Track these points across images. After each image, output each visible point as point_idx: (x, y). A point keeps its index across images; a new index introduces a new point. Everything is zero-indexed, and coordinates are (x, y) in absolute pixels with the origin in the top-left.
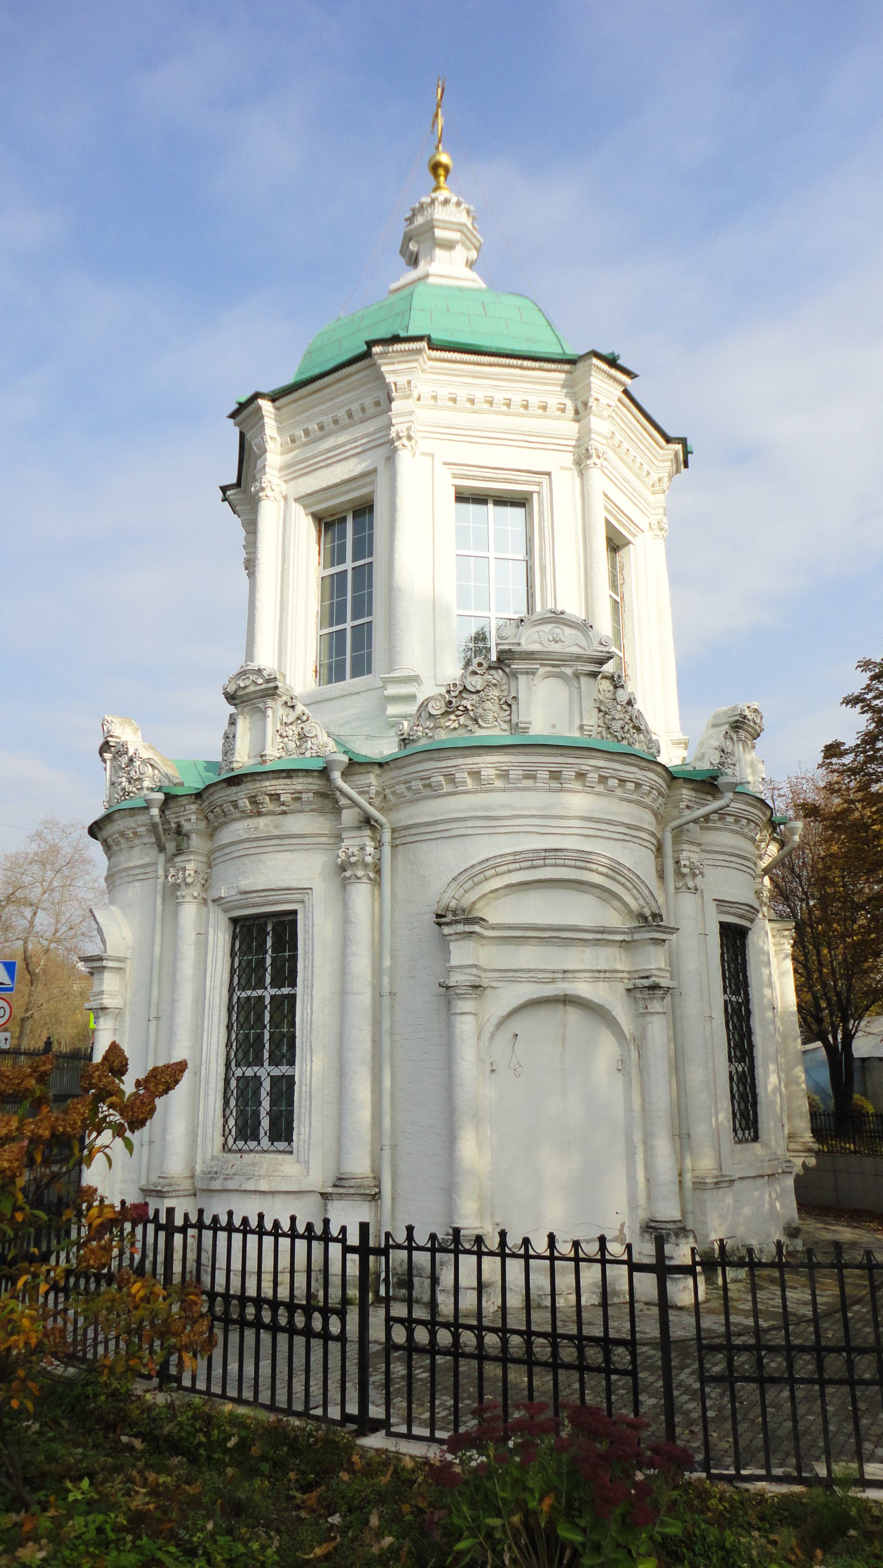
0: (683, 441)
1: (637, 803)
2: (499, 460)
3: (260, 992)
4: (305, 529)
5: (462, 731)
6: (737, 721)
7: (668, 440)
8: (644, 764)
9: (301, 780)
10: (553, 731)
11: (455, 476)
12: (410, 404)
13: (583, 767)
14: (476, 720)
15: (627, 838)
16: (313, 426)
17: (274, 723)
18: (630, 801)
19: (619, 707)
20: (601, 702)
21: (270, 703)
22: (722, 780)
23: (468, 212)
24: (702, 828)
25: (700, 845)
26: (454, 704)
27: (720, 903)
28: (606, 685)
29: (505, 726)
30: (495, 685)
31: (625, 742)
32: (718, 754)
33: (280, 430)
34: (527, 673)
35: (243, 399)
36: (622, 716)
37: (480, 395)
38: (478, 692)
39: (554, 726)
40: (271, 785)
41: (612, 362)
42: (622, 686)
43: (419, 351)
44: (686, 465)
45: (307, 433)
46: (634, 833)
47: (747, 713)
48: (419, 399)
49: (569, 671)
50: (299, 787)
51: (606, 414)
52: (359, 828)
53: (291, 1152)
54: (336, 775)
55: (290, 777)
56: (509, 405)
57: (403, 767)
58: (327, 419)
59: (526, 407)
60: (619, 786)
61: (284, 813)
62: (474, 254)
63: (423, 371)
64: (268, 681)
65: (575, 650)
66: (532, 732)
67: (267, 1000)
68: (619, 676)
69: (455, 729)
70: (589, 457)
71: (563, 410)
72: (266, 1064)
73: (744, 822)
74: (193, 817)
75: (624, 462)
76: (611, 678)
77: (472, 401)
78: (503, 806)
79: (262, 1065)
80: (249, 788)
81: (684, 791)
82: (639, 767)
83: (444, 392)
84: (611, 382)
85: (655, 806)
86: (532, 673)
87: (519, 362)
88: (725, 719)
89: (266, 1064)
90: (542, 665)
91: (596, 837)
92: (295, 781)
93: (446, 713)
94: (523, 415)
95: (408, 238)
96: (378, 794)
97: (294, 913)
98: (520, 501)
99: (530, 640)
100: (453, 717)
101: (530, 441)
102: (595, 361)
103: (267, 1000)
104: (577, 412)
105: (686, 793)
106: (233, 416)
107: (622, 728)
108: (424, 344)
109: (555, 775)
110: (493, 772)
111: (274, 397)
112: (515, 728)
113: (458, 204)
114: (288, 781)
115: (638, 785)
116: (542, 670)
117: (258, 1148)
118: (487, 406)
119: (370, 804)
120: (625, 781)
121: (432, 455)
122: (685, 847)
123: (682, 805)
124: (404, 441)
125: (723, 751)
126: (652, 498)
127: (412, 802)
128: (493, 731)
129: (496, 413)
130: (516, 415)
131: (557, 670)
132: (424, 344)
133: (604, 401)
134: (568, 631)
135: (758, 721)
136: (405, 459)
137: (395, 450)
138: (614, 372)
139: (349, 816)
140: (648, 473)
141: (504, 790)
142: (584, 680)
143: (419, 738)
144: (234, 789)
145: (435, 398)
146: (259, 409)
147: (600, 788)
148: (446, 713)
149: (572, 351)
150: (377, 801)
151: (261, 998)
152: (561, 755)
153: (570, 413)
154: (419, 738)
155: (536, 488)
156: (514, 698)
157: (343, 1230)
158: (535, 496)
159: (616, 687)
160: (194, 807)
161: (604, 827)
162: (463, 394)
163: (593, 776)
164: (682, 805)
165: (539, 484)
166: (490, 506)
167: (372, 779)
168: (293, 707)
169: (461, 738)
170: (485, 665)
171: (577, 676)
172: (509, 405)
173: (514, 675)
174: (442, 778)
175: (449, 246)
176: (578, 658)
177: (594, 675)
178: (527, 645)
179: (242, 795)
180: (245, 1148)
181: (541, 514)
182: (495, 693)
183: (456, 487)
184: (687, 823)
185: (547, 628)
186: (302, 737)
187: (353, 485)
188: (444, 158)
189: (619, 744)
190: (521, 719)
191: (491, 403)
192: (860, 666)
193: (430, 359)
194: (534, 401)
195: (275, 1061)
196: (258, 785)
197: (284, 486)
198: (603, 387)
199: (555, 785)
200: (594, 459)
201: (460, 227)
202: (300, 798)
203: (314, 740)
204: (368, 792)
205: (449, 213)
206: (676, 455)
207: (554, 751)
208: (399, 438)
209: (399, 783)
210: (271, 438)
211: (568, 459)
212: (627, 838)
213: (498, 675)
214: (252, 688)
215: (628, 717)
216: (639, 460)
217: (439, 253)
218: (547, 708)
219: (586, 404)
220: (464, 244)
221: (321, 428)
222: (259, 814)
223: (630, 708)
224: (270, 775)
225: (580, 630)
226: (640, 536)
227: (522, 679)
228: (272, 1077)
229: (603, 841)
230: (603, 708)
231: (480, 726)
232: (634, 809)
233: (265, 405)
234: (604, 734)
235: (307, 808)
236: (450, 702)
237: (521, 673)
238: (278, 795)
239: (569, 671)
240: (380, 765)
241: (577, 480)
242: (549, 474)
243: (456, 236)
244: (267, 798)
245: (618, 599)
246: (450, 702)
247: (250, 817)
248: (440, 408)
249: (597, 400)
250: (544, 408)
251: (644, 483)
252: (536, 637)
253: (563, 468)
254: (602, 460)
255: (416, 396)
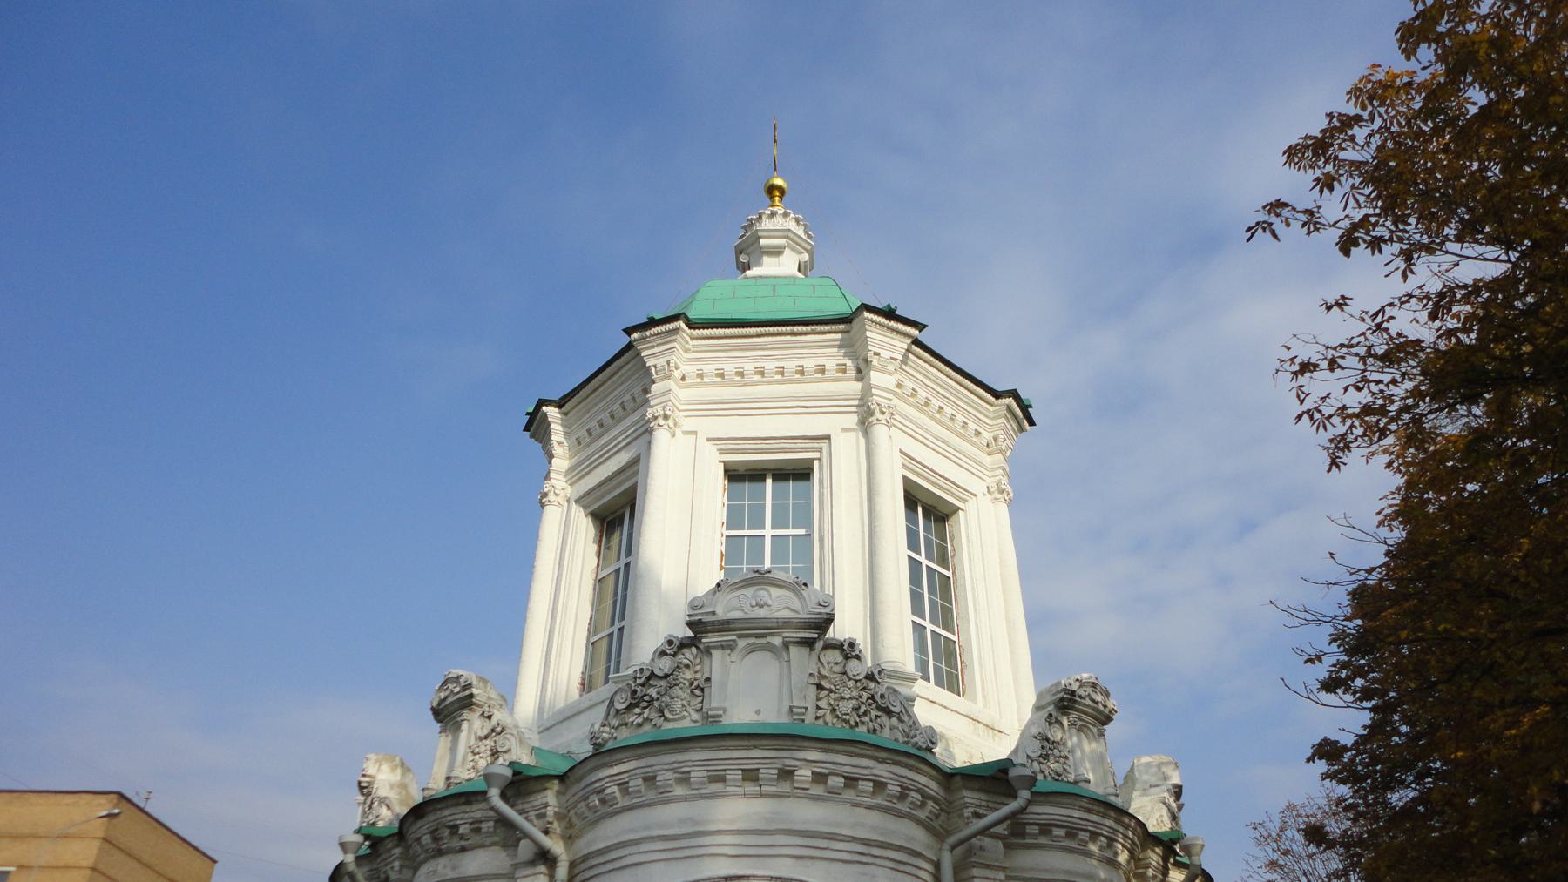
0: (1014, 394)
1: (880, 808)
2: (771, 431)
4: (584, 529)
5: (647, 727)
6: (1062, 699)
7: (997, 395)
8: (883, 755)
9: (480, 806)
10: (756, 718)
11: (722, 452)
12: (671, 384)
13: (788, 762)
14: (661, 711)
15: (864, 859)
16: (593, 424)
17: (469, 738)
18: (869, 807)
19: (851, 684)
20: (825, 677)
21: (466, 714)
22: (1013, 773)
23: (797, 221)
24: (1007, 847)
25: (1004, 869)
26: (639, 693)
28: (836, 656)
29: (695, 716)
30: (687, 666)
31: (863, 729)
32: (1037, 744)
33: (567, 435)
34: (723, 647)
35: (531, 410)
36: (855, 694)
37: (749, 367)
38: (666, 676)
39: (758, 712)
40: (448, 815)
41: (890, 314)
42: (858, 657)
43: (676, 331)
44: (1032, 423)
45: (589, 432)
46: (876, 851)
47: (1075, 687)
48: (683, 379)
49: (777, 641)
50: (478, 815)
51: (891, 368)
52: (532, 863)
54: (494, 793)
55: (468, 803)
56: (782, 374)
57: (581, 779)
58: (605, 416)
59: (802, 373)
60: (846, 786)
61: (463, 849)
62: (806, 257)
63: (687, 351)
64: (465, 688)
65: (787, 614)
66: (725, 720)
68: (852, 645)
69: (640, 725)
70: (871, 414)
71: (844, 371)
73: (1084, 836)
74: (397, 864)
75: (936, 421)
76: (839, 646)
77: (741, 374)
78: (682, 821)
80: (431, 819)
81: (965, 793)
82: (876, 759)
83: (709, 369)
84: (893, 335)
85: (922, 814)
86: (730, 647)
87: (789, 329)
88: (1049, 699)
90: (740, 637)
91: (812, 858)
92: (474, 807)
93: (630, 708)
94: (799, 382)
95: (739, 251)
96: (559, 817)
98: (800, 473)
99: (724, 609)
100: (637, 710)
101: (807, 406)
102: (866, 314)
104: (859, 371)
105: (970, 798)
106: (527, 429)
107: (856, 709)
108: (681, 324)
109: (751, 776)
110: (669, 775)
111: (560, 404)
112: (709, 718)
113: (786, 215)
114: (467, 808)
115: (879, 786)
116: (742, 643)
118: (758, 377)
119: (546, 832)
120: (857, 779)
121: (695, 433)
122: (975, 872)
123: (968, 812)
124: (661, 421)
125: (1048, 740)
126: (987, 460)
127: (595, 823)
128: (686, 722)
129: (769, 383)
130: (791, 382)
131: (763, 641)
132: (681, 324)
133: (885, 354)
134: (775, 592)
135: (1099, 698)
136: (661, 438)
137: (650, 431)
138: (893, 324)
139: (525, 850)
140: (978, 433)
141: (686, 799)
142: (793, 649)
143: (606, 741)
145: (700, 376)
146: (545, 415)
147: (818, 790)
148: (630, 708)
149: (843, 309)
150: (557, 827)
152: (755, 747)
153: (852, 372)
154: (606, 741)
155: (816, 455)
156: (708, 680)
158: (816, 463)
159: (847, 658)
160: (397, 851)
161: (824, 843)
162: (730, 368)
163: (804, 774)
164: (968, 812)
165: (819, 450)
166: (769, 481)
167: (550, 797)
168: (489, 717)
169: (647, 733)
170: (676, 643)
171: (786, 645)
172: (782, 374)
173: (707, 652)
174: (615, 789)
175: (776, 252)
176: (787, 624)
177: (809, 643)
178: (722, 614)
179: (424, 830)
181: (821, 481)
182: (688, 675)
183: (725, 463)
184: (974, 835)
185: (749, 592)
186: (495, 753)
187: (623, 476)
188: (778, 182)
189: (859, 732)
190: (714, 705)
191: (762, 373)
192: (1335, 640)
193: (692, 338)
194: (810, 365)
196: (439, 814)
197: (569, 489)
198: (884, 342)
199: (751, 788)
200: (878, 415)
201: (786, 233)
202: (478, 830)
203: (506, 756)
204: (543, 816)
205: (778, 223)
206: (1009, 408)
207: (745, 743)
208: (655, 418)
209: (578, 802)
210: (559, 443)
211: (852, 420)
212: (864, 859)
213: (689, 655)
214: (450, 700)
215: (865, 695)
216: (959, 418)
217: (766, 259)
218: (750, 692)
219: (866, 360)
220: (793, 249)
221: (601, 426)
222: (440, 853)
223: (872, 685)
224: (450, 802)
225: (793, 591)
226: (972, 502)
227: (716, 654)
229: (825, 863)
230: (825, 684)
231: (666, 719)
232: (875, 818)
233: (552, 412)
234: (829, 718)
235: (488, 841)
236: (635, 692)
237: (716, 648)
238: (457, 826)
239: (777, 641)
240: (562, 778)
241: (862, 441)
242: (828, 438)
243: (782, 241)
244: (447, 831)
245: (949, 574)
246: (635, 692)
247: (433, 857)
248: (708, 385)
249: (877, 354)
250: (823, 371)
251: (973, 443)
252: (735, 603)
253: (844, 430)
254: (887, 416)
255: (677, 374)
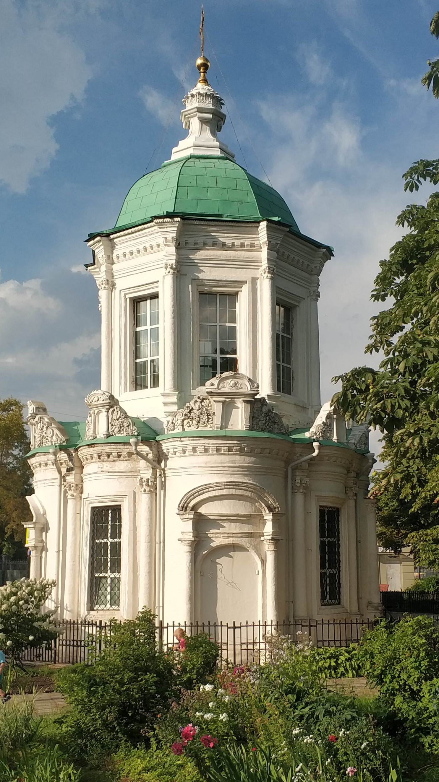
3: (105, 540)
27: (319, 497)
53: (118, 610)
67: (109, 544)
72: (109, 572)
79: (107, 573)
89: (109, 572)
97: (120, 505)
103: (109, 544)
117: (105, 608)
144: (92, 449)
151: (107, 543)
157: (96, 622)
180: (100, 608)
195: (112, 572)
215: (268, 418)
228: (111, 578)
